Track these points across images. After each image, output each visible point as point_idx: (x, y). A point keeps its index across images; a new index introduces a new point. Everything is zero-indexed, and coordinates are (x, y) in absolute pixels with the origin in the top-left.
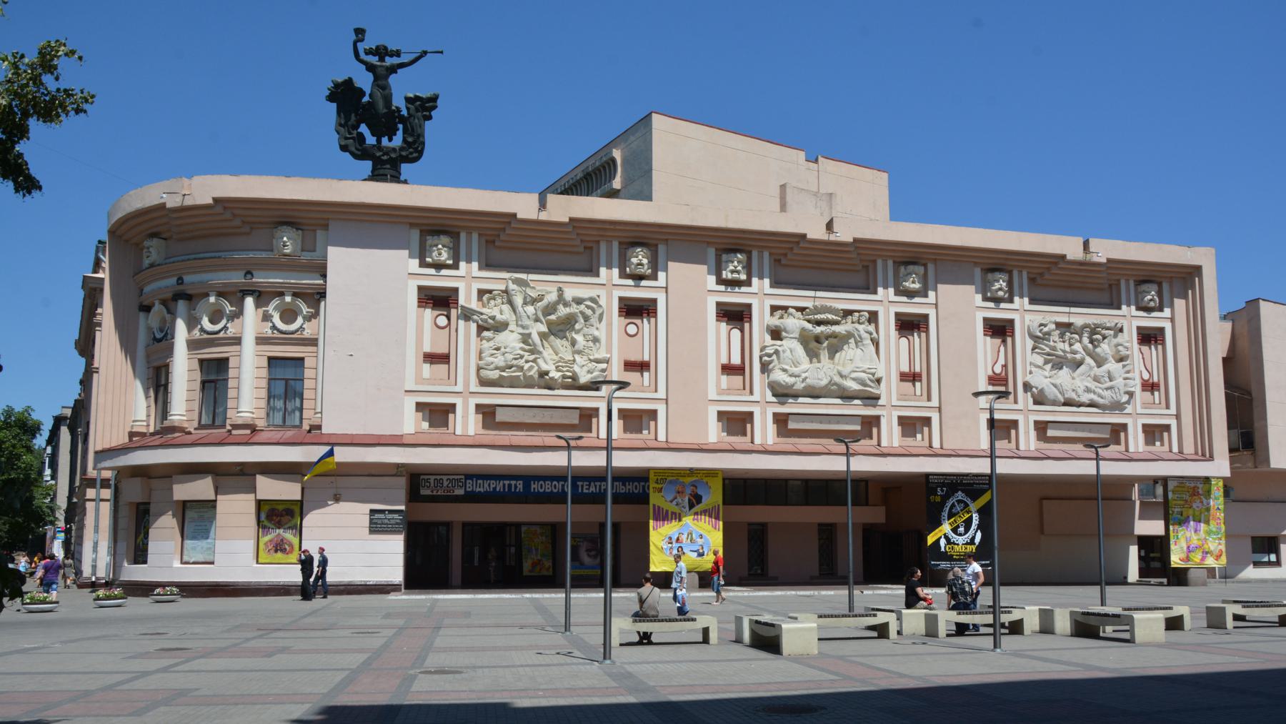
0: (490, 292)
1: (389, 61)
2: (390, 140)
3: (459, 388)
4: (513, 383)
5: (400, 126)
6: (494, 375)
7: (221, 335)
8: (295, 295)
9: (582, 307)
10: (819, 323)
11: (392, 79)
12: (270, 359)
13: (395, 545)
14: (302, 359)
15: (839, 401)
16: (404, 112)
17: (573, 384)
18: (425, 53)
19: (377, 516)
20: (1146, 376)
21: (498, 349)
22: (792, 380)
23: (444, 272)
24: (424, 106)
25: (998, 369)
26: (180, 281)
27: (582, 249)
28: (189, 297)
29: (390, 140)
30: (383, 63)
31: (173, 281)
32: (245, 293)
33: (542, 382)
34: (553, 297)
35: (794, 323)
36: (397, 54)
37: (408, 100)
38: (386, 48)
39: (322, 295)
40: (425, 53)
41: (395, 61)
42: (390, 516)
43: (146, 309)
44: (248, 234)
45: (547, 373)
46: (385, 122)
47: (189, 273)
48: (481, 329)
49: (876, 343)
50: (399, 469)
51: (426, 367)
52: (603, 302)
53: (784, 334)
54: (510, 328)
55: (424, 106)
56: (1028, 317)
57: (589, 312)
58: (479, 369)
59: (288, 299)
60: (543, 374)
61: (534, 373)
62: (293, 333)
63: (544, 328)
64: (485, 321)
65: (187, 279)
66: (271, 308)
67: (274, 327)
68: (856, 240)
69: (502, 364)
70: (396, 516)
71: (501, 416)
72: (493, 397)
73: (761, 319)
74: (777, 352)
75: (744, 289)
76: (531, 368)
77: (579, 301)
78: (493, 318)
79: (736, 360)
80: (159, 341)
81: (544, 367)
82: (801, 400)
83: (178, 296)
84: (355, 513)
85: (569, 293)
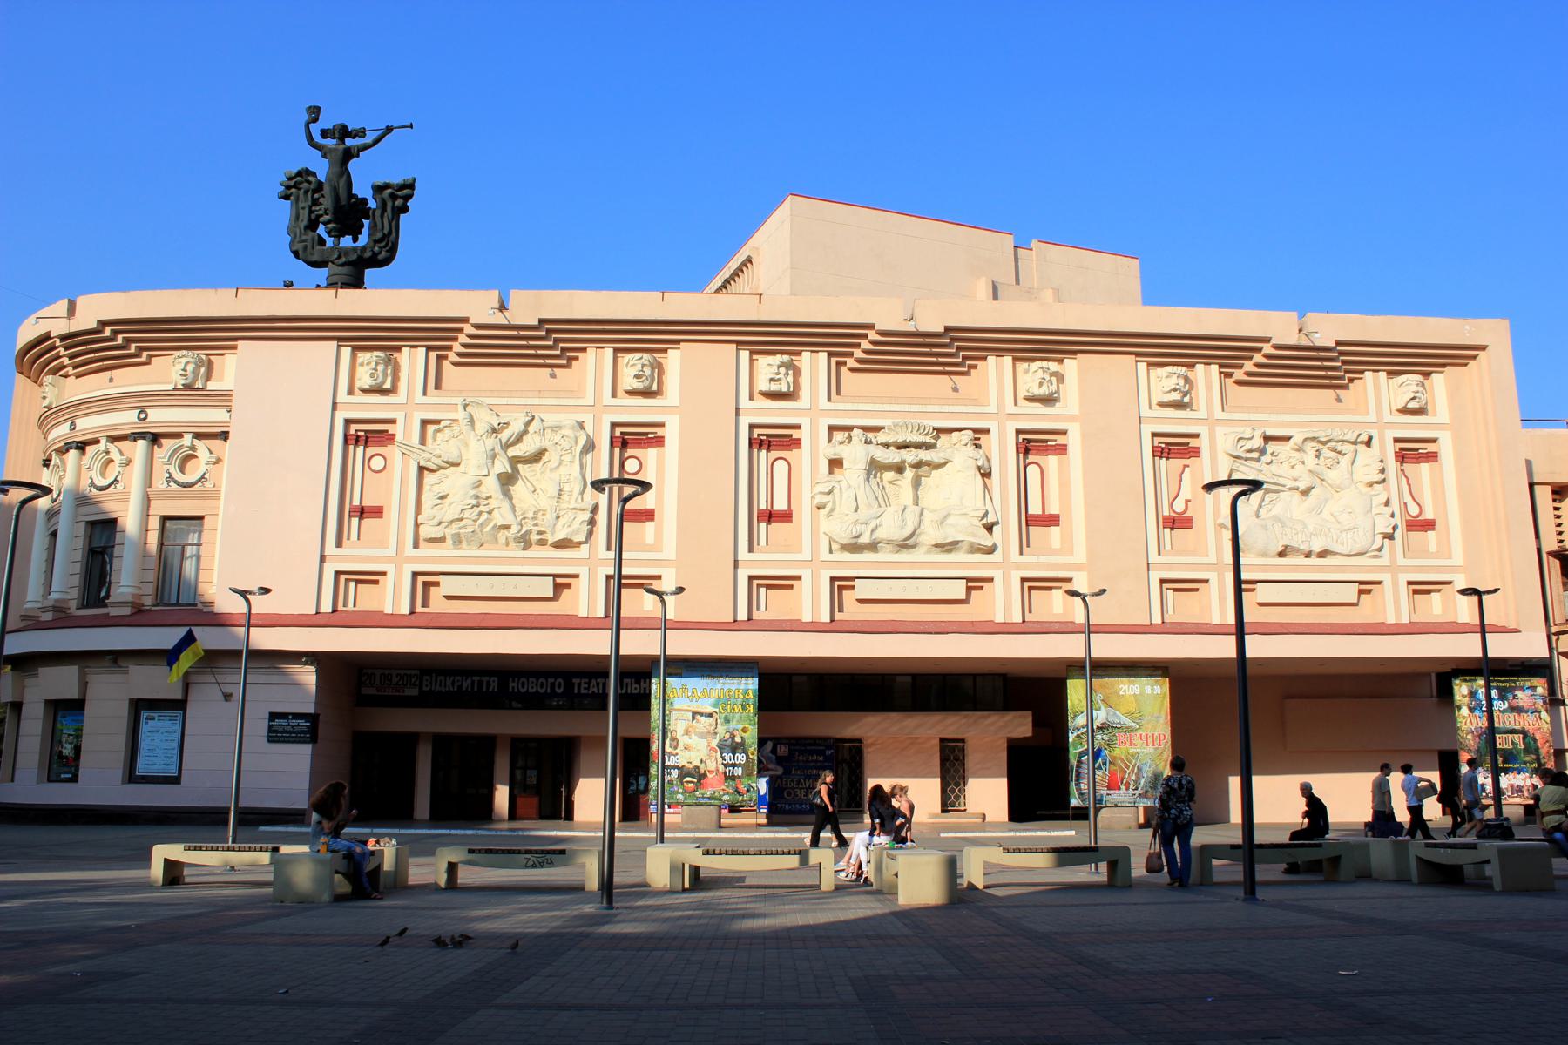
0: (438, 422)
1: (349, 142)
2: (355, 240)
3: (391, 551)
5: (366, 223)
7: (111, 489)
9: (557, 438)
11: (352, 165)
14: (201, 518)
16: (372, 204)
18: (389, 130)
19: (277, 722)
20: (1414, 510)
21: (442, 498)
24: (398, 197)
25: (1179, 506)
29: (355, 240)
30: (344, 144)
34: (516, 427)
35: (856, 453)
36: (361, 133)
37: (378, 189)
38: (344, 127)
39: (225, 436)
40: (389, 130)
41: (358, 141)
42: (295, 722)
46: (349, 214)
49: (986, 475)
52: (589, 427)
53: (845, 464)
54: (461, 468)
55: (398, 197)
56: (1220, 430)
58: (417, 525)
62: (192, 485)
63: (502, 466)
68: (948, 329)
69: (448, 518)
70: (302, 722)
72: (431, 559)
76: (488, 521)
77: (555, 429)
79: (780, 505)
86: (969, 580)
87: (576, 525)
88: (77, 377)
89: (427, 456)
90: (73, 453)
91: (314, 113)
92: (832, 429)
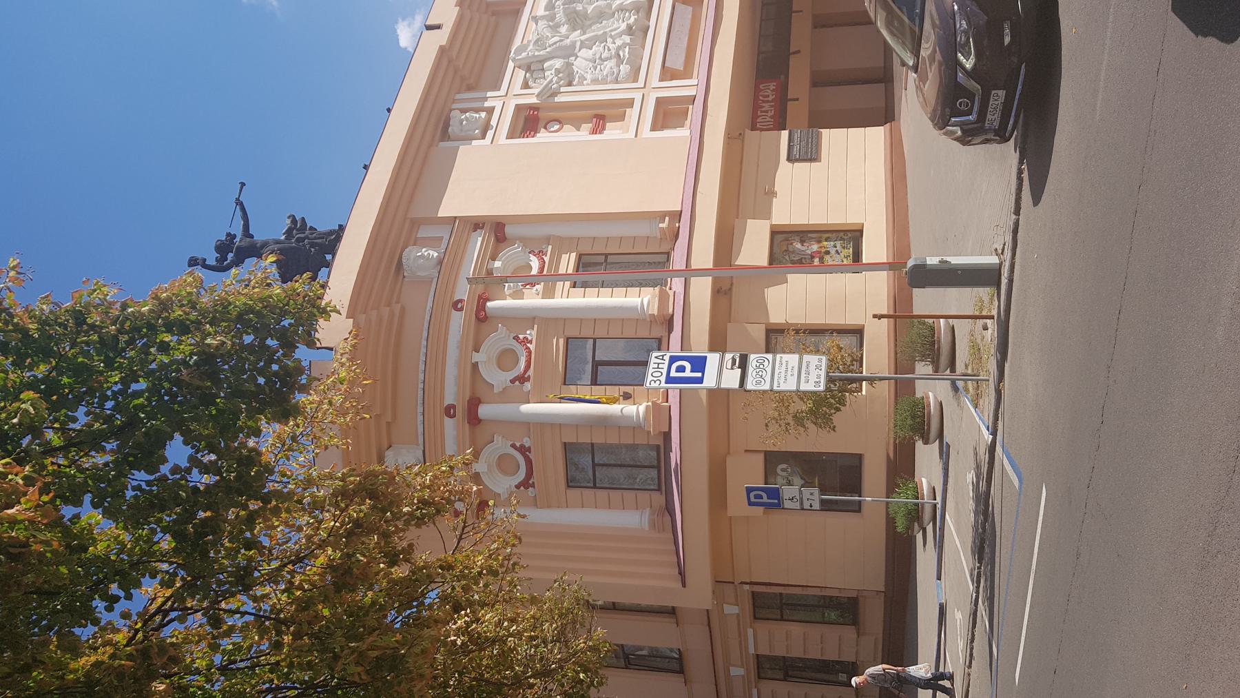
6: (625, 68)
7: (532, 347)
8: (494, 259)
13: (831, 138)
23: (493, 122)
26: (449, 411)
28: (474, 403)
31: (449, 422)
32: (482, 317)
33: (641, 34)
39: (498, 231)
44: (403, 309)
45: (630, 27)
47: (442, 398)
48: (570, 84)
50: (734, 138)
58: (617, 81)
59: (498, 264)
60: (630, 30)
61: (627, 39)
65: (449, 400)
69: (614, 61)
71: (677, 62)
80: (529, 463)
81: (623, 26)
83: (473, 419)
84: (789, 176)
85: (541, 11)
88: (394, 416)
89: (555, 79)
90: (484, 411)
91: (193, 262)
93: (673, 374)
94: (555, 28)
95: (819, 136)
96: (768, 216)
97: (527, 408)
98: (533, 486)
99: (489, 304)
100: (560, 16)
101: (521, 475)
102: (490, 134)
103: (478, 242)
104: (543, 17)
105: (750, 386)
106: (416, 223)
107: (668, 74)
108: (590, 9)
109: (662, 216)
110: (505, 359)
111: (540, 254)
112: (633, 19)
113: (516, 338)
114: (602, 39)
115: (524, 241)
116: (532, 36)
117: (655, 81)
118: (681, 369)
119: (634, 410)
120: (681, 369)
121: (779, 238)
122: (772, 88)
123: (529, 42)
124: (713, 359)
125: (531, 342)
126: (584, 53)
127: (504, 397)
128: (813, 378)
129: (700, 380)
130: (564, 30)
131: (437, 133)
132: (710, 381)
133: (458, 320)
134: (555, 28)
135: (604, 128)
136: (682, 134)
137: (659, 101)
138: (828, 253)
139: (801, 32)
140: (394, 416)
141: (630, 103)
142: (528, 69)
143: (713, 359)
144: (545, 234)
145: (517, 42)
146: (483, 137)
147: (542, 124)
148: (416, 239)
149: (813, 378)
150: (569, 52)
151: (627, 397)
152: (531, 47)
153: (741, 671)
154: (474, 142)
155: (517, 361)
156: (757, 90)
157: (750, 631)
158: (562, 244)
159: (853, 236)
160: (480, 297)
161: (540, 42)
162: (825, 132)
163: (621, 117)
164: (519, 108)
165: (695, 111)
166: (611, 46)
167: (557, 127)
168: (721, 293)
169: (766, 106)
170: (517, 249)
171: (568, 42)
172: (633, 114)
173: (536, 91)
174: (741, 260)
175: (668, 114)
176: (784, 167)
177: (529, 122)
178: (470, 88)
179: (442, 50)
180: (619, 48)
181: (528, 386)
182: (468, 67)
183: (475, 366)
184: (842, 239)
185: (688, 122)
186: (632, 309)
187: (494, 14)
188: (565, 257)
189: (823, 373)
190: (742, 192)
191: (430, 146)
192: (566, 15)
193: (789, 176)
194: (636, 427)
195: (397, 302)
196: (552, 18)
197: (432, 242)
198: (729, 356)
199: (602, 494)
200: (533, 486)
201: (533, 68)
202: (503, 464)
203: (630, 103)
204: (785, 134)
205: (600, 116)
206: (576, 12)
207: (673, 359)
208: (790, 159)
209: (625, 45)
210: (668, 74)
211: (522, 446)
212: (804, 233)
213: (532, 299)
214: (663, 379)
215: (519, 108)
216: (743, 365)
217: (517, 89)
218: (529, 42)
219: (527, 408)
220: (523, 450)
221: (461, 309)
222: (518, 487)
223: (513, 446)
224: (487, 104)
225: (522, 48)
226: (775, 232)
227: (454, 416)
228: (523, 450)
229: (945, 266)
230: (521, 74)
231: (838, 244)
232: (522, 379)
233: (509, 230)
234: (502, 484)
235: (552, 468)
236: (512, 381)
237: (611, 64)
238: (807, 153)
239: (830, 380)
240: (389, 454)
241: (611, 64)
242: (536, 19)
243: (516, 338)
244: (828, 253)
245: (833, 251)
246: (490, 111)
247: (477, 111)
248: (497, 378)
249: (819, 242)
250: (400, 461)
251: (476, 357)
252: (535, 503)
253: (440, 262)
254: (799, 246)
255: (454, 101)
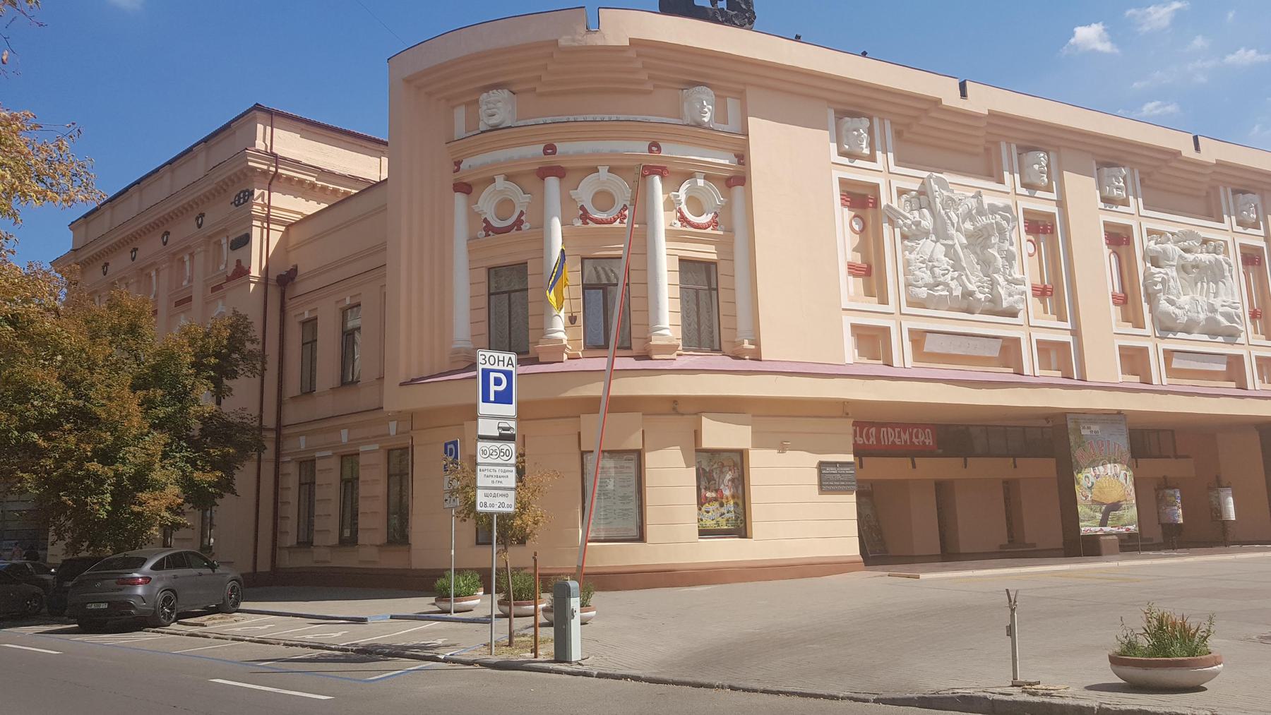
4: (937, 303)
6: (923, 293)
7: (617, 224)
8: (706, 178)
10: (1186, 250)
12: (681, 260)
13: (847, 504)
15: (1206, 337)
17: (995, 309)
22: (1177, 311)
23: (858, 163)
26: (550, 149)
27: (981, 150)
28: (559, 172)
33: (964, 306)
39: (737, 179)
42: (843, 470)
43: (464, 188)
44: (649, 93)
45: (971, 294)
47: (562, 140)
48: (904, 237)
50: (843, 408)
51: (851, 278)
57: (1004, 223)
58: (908, 285)
59: (701, 182)
60: (968, 294)
61: (958, 292)
64: (909, 227)
65: (560, 147)
66: (682, 194)
67: (683, 219)
69: (931, 281)
71: (931, 345)
73: (1141, 244)
74: (1164, 282)
75: (1121, 208)
77: (994, 209)
78: (918, 224)
81: (971, 287)
82: (1180, 335)
83: (544, 173)
84: (803, 465)
85: (987, 200)
86: (1230, 356)
87: (1017, 297)
88: (542, 95)
89: (909, 222)
90: (552, 183)
92: (1150, 232)
93: (492, 375)
94: (969, 216)
95: (848, 492)
96: (758, 445)
97: (556, 226)
98: (487, 235)
99: (657, 178)
100: (983, 221)
101: (497, 223)
102: (845, 161)
103: (724, 160)
104: (980, 203)
105: (481, 445)
106: (741, 95)
107: (918, 337)
108: (993, 251)
109: (756, 342)
110: (604, 198)
111: (714, 224)
112: (982, 296)
113: (625, 208)
114: (957, 266)
115: (728, 207)
116: (958, 193)
117: (908, 324)
118: (498, 382)
119: (559, 328)
120: (498, 382)
121: (737, 458)
122: (927, 442)
123: (952, 191)
124: (510, 410)
125: (622, 222)
126: (940, 250)
127: (567, 201)
128: (489, 501)
129: (486, 399)
130: (968, 226)
131: (845, 107)
132: (484, 408)
133: (640, 148)
134: (969, 216)
135: (855, 276)
136: (849, 353)
137: (886, 331)
138: (722, 505)
139: (998, 468)
140: (542, 95)
141: (883, 301)
142: (921, 193)
143: (510, 410)
144: (733, 226)
145: (947, 177)
146: (841, 154)
147: (859, 212)
148: (724, 97)
149: (489, 501)
150: (940, 233)
151: (572, 320)
152: (945, 193)
153: (345, 439)
154: (834, 146)
155: (603, 211)
156: (924, 426)
157: (376, 447)
158: (725, 245)
159: (740, 529)
160: (664, 168)
161: (950, 202)
162: (853, 497)
163: (869, 293)
164: (876, 187)
165: (877, 367)
166: (949, 277)
167: (857, 228)
168: (675, 405)
169: (906, 437)
170: (719, 200)
171: (952, 231)
172: (873, 304)
173: (895, 205)
174: (706, 422)
175: (872, 340)
176: (816, 458)
177: (860, 199)
178: (898, 134)
179: (937, 102)
180: (947, 285)
181: (579, 223)
182: (925, 134)
183: (596, 170)
184: (737, 518)
185: (865, 360)
186: (657, 321)
187: (987, 150)
188: (712, 248)
189: (496, 509)
190: (781, 420)
191: (829, 101)
192: (985, 227)
193: (803, 465)
194: (543, 330)
195: (655, 86)
196: (981, 212)
197: (721, 115)
198: (513, 424)
199: (483, 302)
200: (487, 235)
201: (923, 197)
202: (505, 205)
203: (883, 301)
204: (850, 458)
205: (869, 272)
206: (989, 236)
207: (508, 375)
208: (822, 465)
209: (950, 290)
210: (918, 337)
211: (522, 222)
212: (741, 481)
213: (663, 220)
214: (488, 366)
215: (876, 187)
216: (502, 438)
217: (897, 183)
218: (952, 191)
219: (556, 226)
220: (518, 223)
221: (651, 151)
222: (485, 220)
223: (522, 213)
224: (879, 154)
225: (943, 184)
226: (742, 454)
227: (545, 153)
228: (518, 223)
229: (569, 615)
230: (915, 186)
231: (732, 515)
232: (585, 217)
233: (738, 190)
234: (487, 204)
235: (505, 252)
236: (582, 208)
237: (928, 278)
238: (828, 480)
239: (489, 516)
240: (504, 94)
241: (928, 278)
242: (978, 195)
243: (625, 208)
244: (722, 505)
245: (723, 510)
246: (872, 158)
247: (871, 145)
248: (585, 193)
249: (733, 497)
250: (499, 105)
251: (603, 171)
252: (472, 238)
253: (699, 125)
254: (728, 477)
255: (882, 119)
